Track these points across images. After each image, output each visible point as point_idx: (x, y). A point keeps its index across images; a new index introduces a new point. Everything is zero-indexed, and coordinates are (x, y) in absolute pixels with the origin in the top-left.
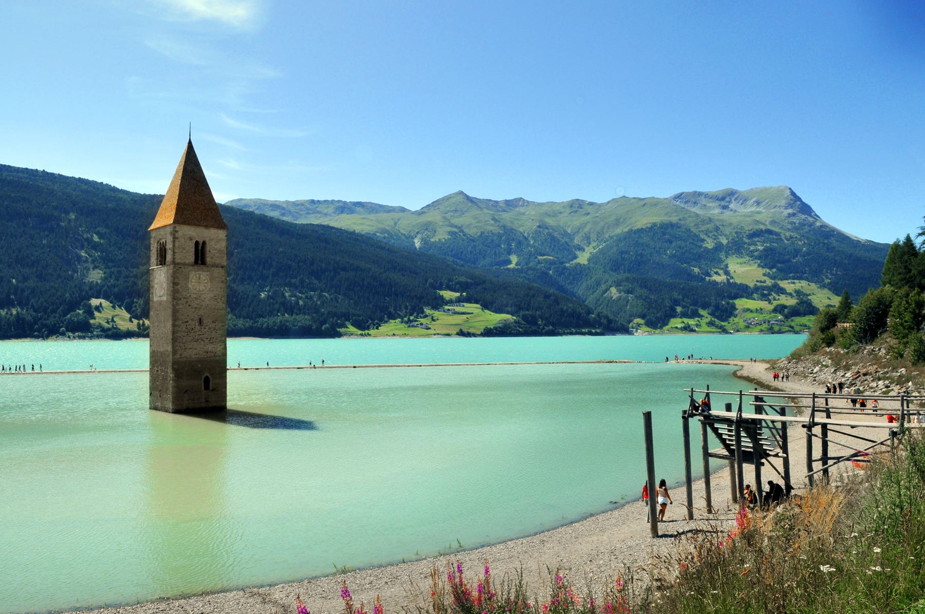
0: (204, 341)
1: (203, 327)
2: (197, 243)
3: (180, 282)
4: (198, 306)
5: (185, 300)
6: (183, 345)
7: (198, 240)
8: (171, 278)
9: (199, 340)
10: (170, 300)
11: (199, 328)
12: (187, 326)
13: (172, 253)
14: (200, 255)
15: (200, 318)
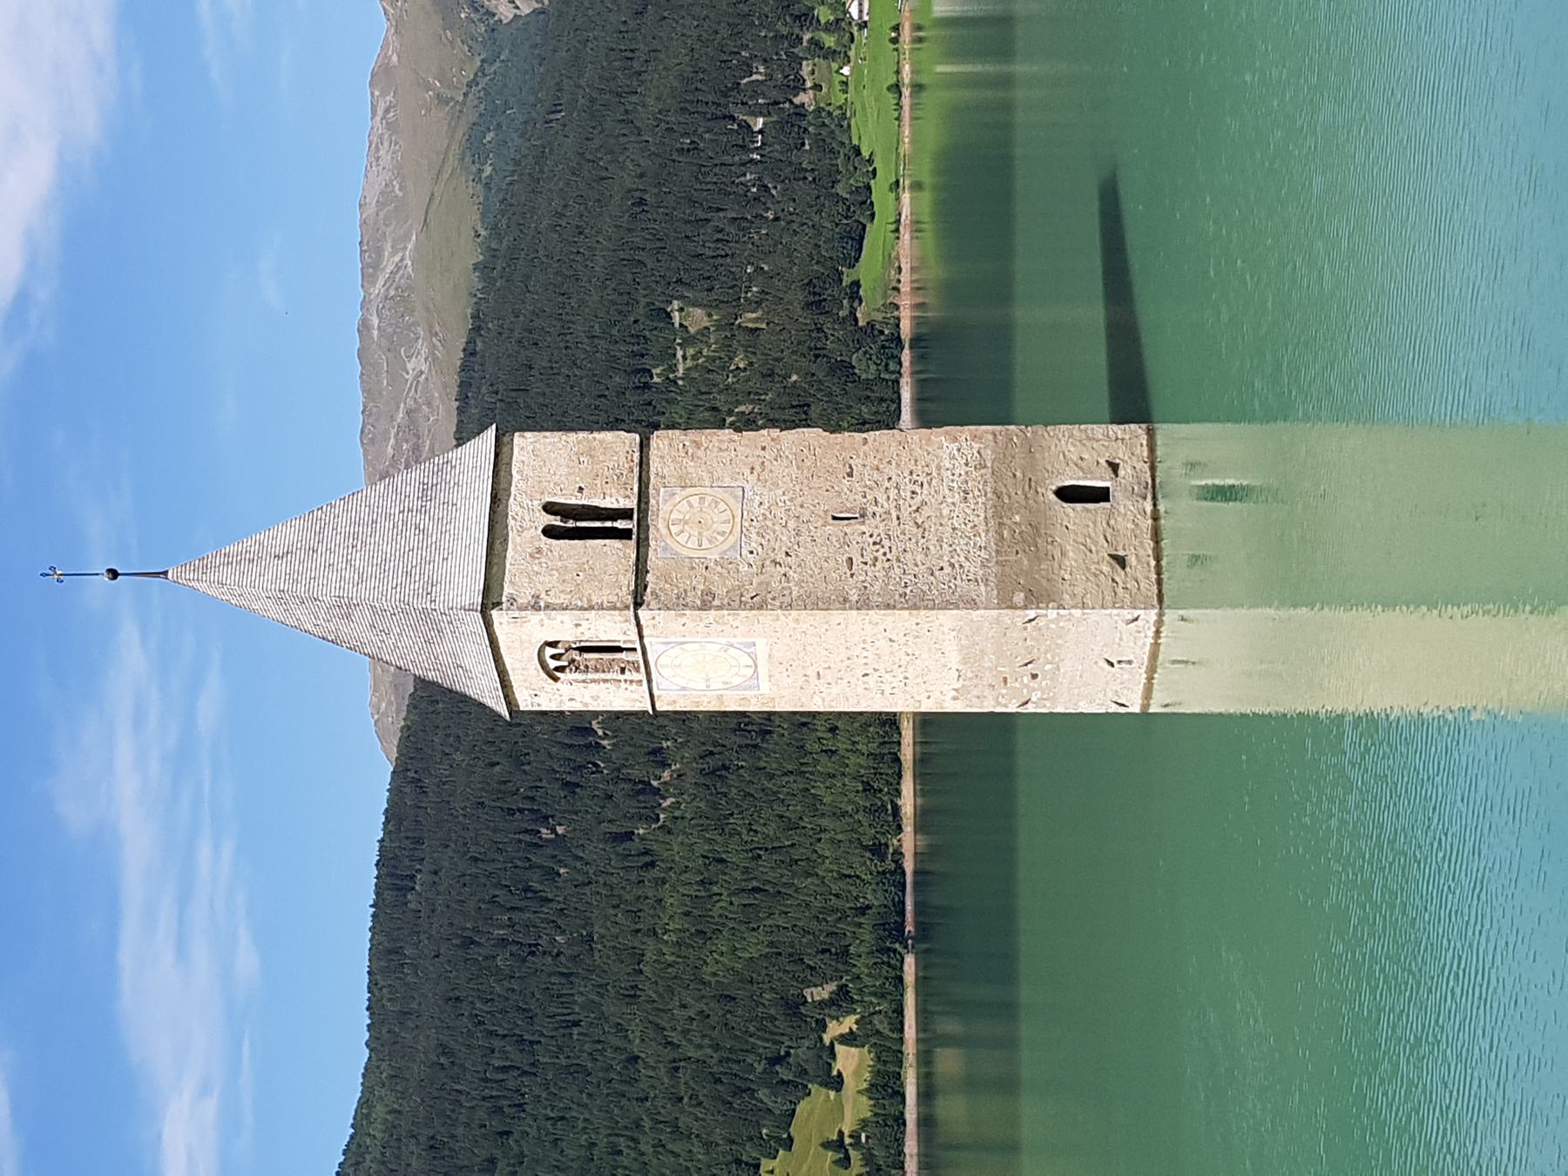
0: (924, 503)
1: (870, 510)
2: (550, 532)
3: (701, 587)
4: (792, 525)
5: (769, 568)
6: (937, 573)
7: (541, 528)
8: (684, 620)
9: (920, 521)
10: (766, 617)
11: (870, 521)
12: (866, 563)
13: (587, 614)
14: (597, 524)
15: (834, 518)
